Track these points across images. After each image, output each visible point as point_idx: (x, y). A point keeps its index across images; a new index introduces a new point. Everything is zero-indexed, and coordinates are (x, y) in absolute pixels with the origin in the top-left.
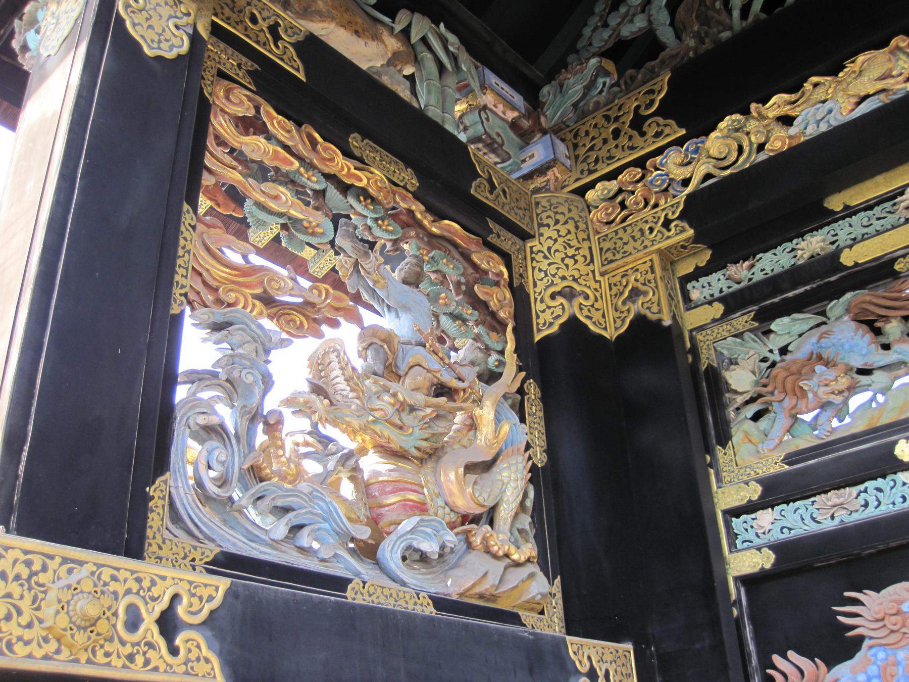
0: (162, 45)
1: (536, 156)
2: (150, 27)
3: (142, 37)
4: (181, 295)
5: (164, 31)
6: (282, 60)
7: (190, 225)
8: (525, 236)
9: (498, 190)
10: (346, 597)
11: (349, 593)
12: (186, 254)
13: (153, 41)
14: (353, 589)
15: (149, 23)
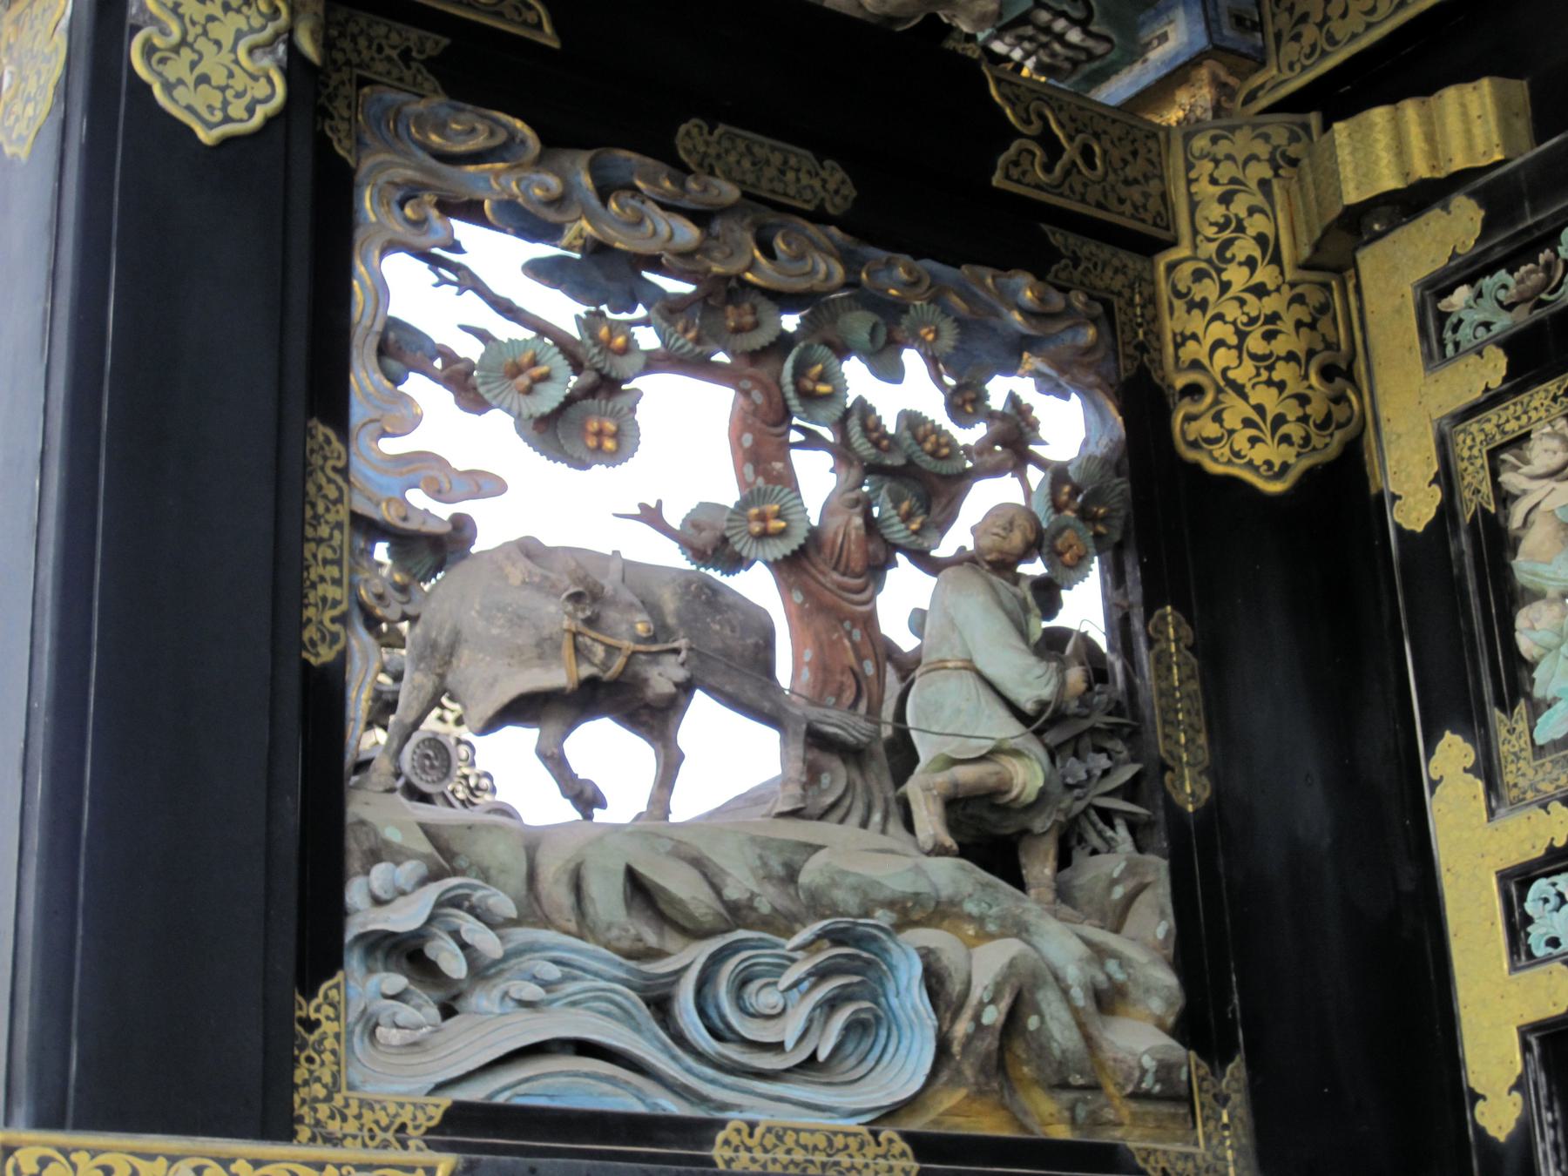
0: (232, 111)
1: (1171, 36)
2: (204, 79)
3: (189, 108)
4: (333, 620)
5: (231, 75)
6: (499, 15)
7: (335, 469)
8: (1151, 246)
9: (1070, 151)
10: (711, 1162)
11: (718, 1153)
12: (337, 533)
13: (211, 108)
14: (727, 1142)
15: (198, 71)
